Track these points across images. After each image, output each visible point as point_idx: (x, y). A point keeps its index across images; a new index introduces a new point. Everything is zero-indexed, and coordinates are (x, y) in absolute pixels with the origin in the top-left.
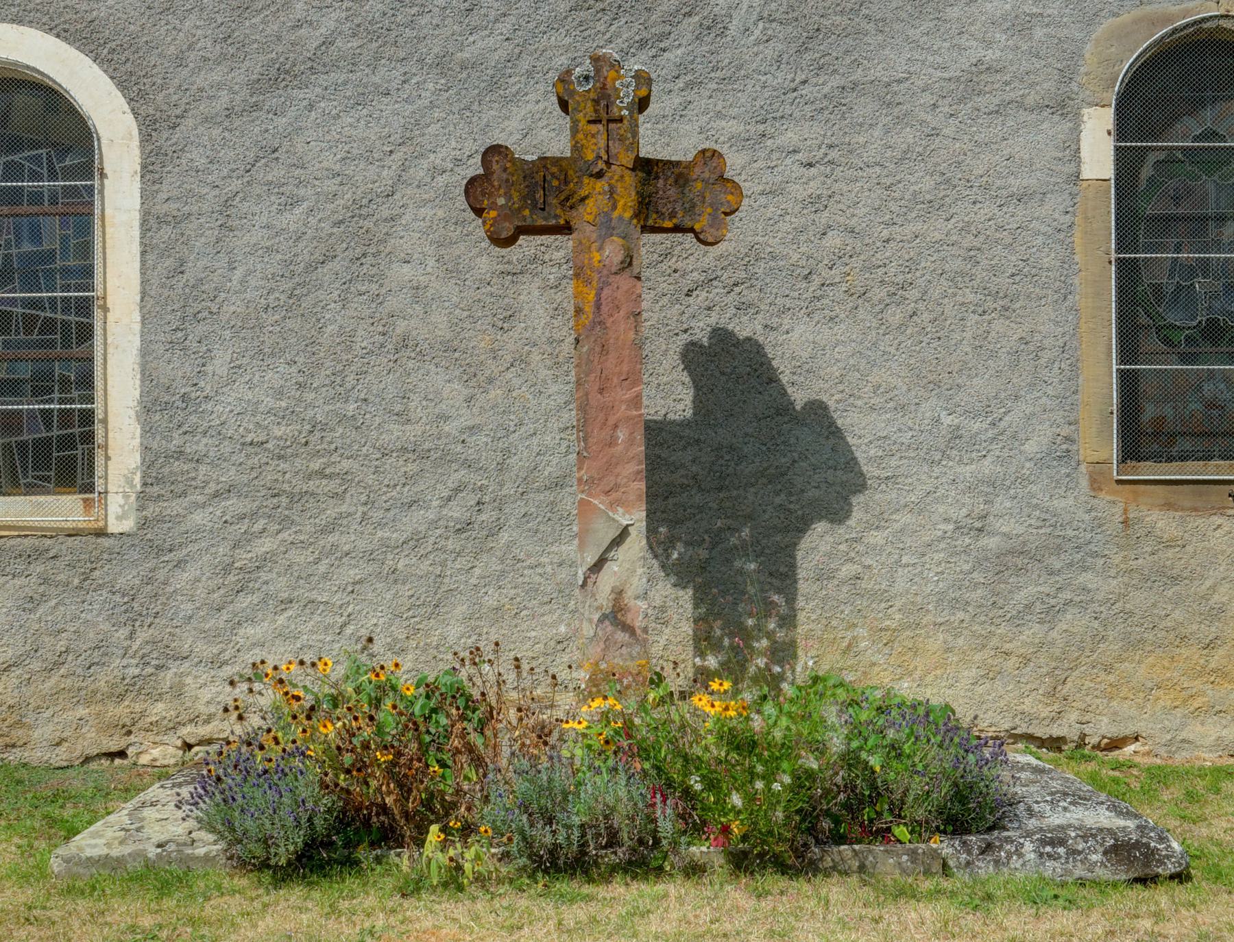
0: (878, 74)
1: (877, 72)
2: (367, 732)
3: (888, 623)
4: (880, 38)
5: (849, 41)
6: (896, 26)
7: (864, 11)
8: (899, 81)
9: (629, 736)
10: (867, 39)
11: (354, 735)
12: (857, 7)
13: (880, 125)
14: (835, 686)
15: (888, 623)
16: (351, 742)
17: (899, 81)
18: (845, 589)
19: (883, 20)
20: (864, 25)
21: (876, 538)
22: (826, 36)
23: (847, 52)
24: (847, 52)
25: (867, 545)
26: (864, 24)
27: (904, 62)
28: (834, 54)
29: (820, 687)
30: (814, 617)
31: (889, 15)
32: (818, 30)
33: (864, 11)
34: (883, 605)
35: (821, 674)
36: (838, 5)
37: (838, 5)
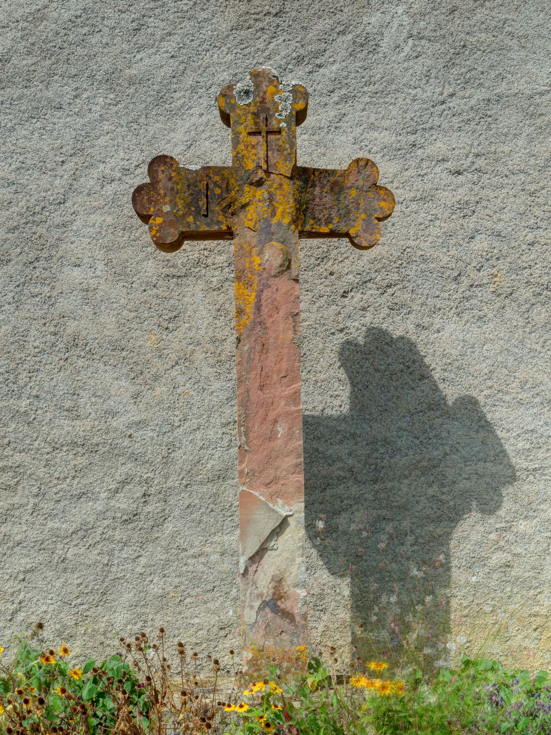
0: (521, 87)
1: (521, 86)
2: (37, 715)
3: (537, 609)
4: (523, 53)
5: (493, 56)
6: (538, 43)
7: (508, 29)
8: (541, 94)
9: (288, 718)
10: (511, 55)
11: (24, 718)
12: (500, 25)
13: (524, 134)
14: (486, 670)
15: (537, 609)
16: (21, 725)
17: (541, 94)
18: (495, 576)
19: (526, 37)
20: (507, 41)
21: (522, 526)
22: (472, 52)
23: (492, 67)
24: (492, 67)
25: (516, 534)
26: (507, 41)
27: (545, 76)
28: (480, 69)
29: (472, 671)
30: (465, 603)
31: (531, 32)
32: (464, 46)
33: (508, 29)
34: (532, 592)
35: (472, 658)
36: (483, 23)
37: (483, 23)
